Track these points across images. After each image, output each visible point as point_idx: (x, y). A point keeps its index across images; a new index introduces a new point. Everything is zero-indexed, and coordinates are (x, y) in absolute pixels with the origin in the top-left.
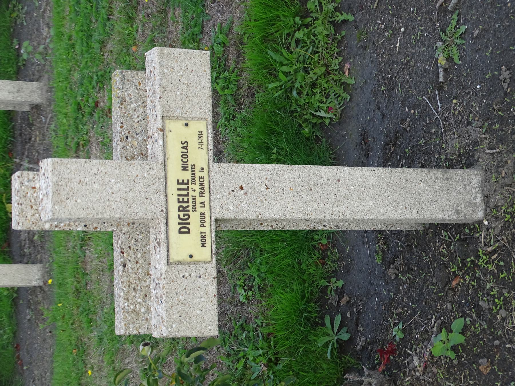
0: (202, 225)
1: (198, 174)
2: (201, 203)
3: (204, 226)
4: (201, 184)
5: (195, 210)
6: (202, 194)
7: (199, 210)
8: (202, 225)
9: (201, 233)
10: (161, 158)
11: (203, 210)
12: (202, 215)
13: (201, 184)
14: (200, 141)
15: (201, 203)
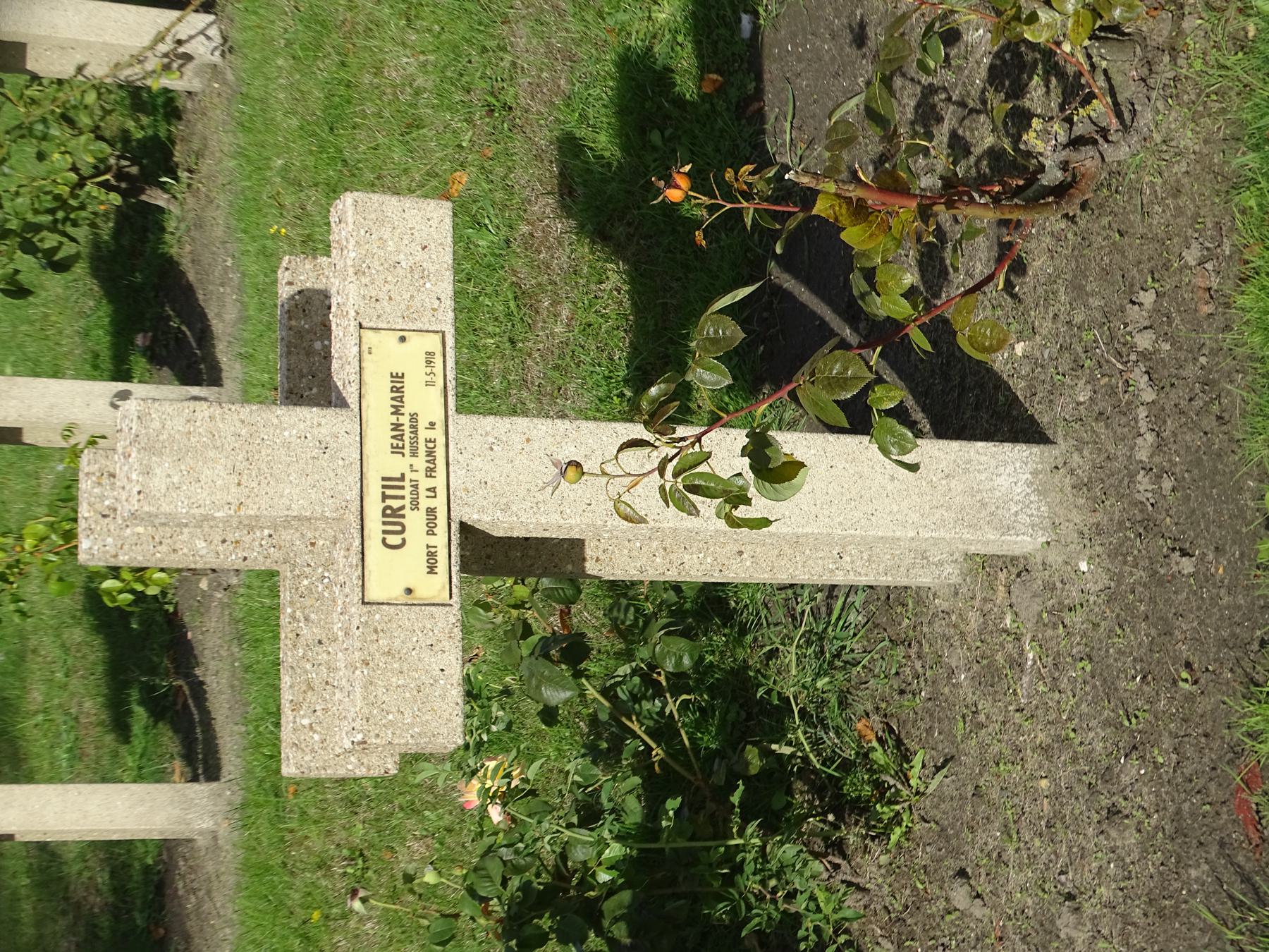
0: (431, 532)
1: (423, 434)
2: (428, 490)
3: (434, 534)
4: (430, 453)
5: (415, 505)
6: (430, 472)
7: (424, 503)
8: (431, 532)
9: (428, 547)
10: (357, 410)
11: (432, 503)
12: (431, 511)
13: (430, 453)
14: (428, 370)
15: (428, 490)
